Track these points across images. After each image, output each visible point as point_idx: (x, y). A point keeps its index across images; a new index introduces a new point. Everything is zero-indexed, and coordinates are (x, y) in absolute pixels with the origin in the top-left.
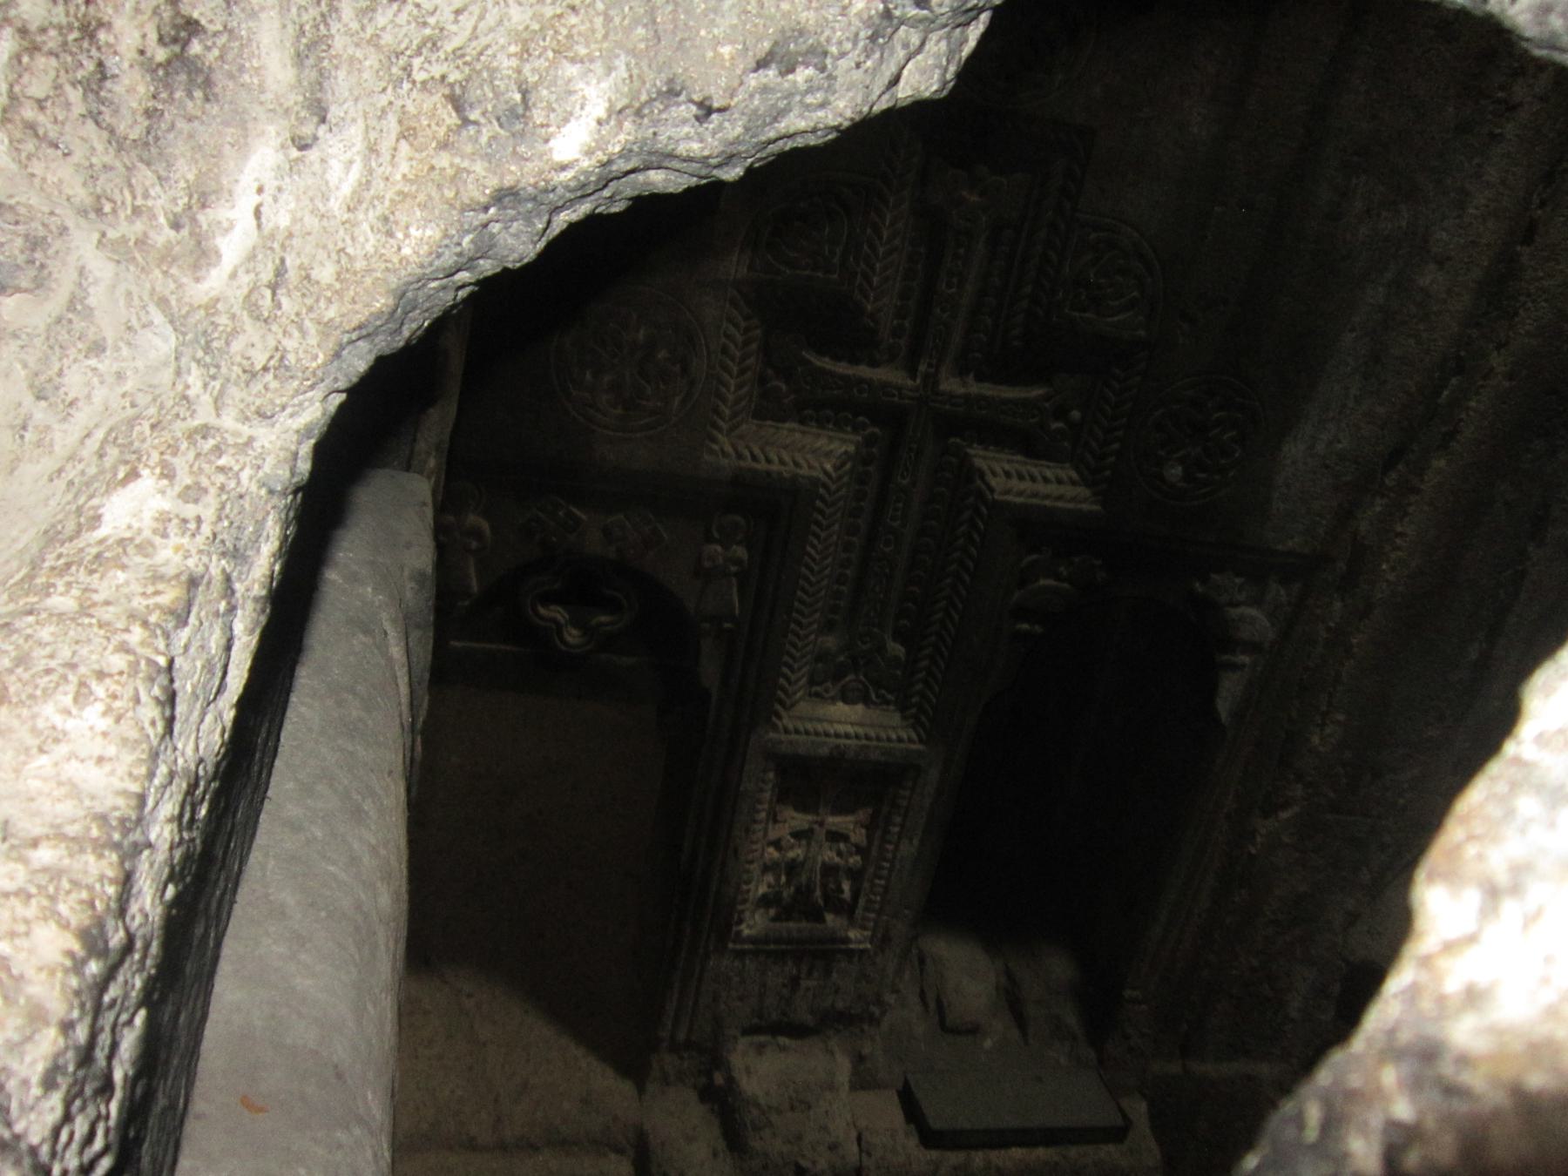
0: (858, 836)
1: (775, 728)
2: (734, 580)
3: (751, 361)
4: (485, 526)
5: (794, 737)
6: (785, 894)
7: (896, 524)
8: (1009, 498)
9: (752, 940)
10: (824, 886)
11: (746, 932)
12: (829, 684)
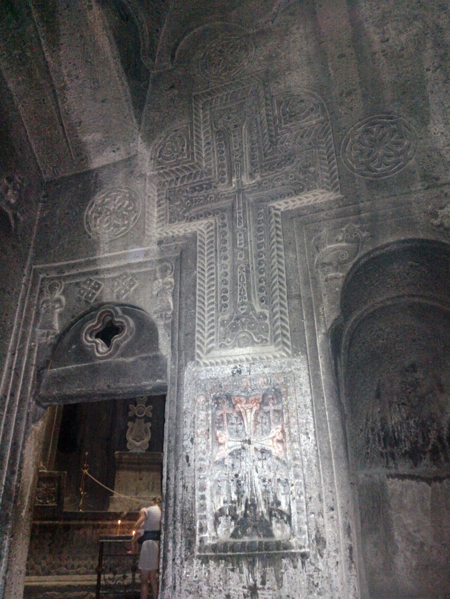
0: (277, 449)
1: (198, 363)
2: (170, 295)
3: (162, 202)
4: (63, 299)
5: (209, 368)
6: (238, 512)
7: (242, 246)
8: (290, 208)
9: (214, 548)
10: (266, 501)
11: (209, 542)
12: (230, 340)
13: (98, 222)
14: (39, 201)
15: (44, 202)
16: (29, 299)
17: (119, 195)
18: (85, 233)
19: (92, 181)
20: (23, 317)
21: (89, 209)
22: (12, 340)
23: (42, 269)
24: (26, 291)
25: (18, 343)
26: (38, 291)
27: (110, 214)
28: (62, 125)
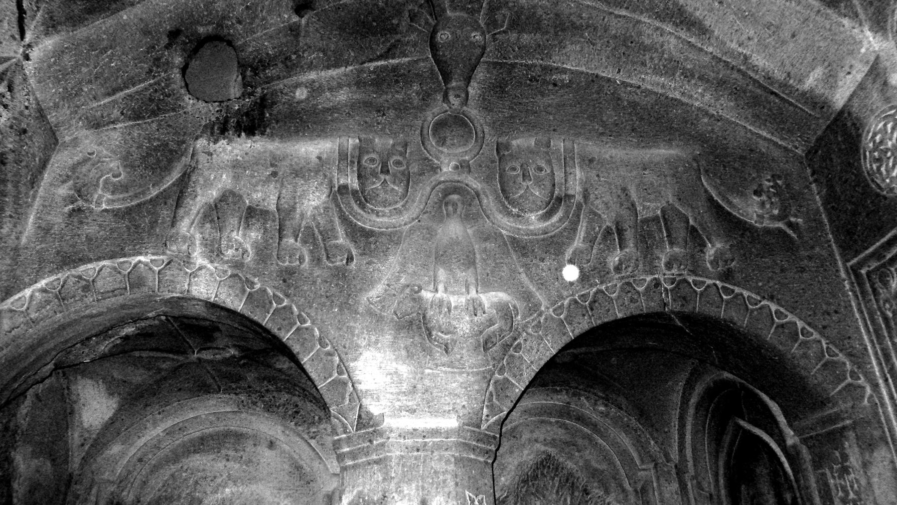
13: (884, 173)
14: (811, 183)
15: (816, 181)
16: (866, 306)
17: (889, 122)
18: (878, 195)
19: (849, 124)
20: (871, 330)
21: (865, 162)
22: (874, 362)
23: (858, 263)
24: (856, 296)
25: (884, 365)
26: (870, 290)
27: (893, 154)
28: (773, 93)
